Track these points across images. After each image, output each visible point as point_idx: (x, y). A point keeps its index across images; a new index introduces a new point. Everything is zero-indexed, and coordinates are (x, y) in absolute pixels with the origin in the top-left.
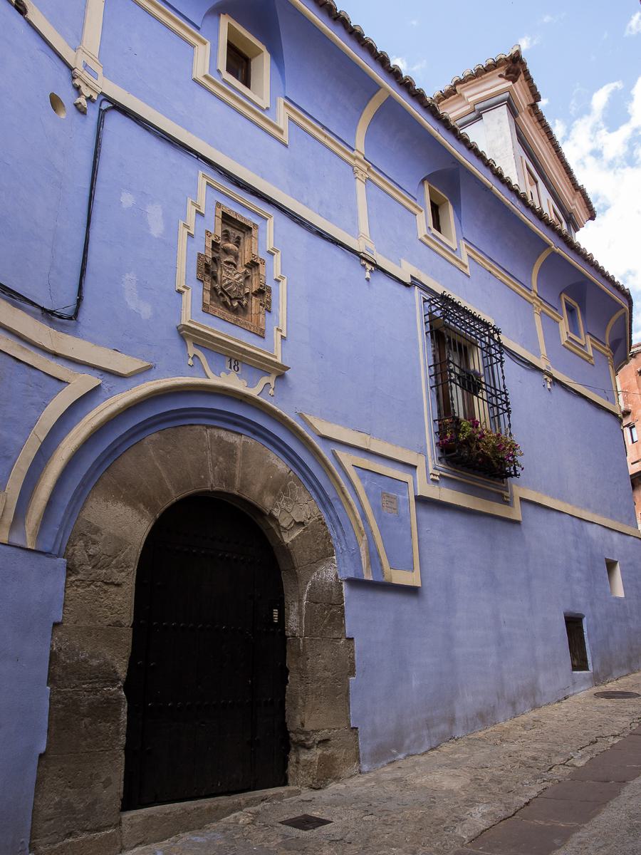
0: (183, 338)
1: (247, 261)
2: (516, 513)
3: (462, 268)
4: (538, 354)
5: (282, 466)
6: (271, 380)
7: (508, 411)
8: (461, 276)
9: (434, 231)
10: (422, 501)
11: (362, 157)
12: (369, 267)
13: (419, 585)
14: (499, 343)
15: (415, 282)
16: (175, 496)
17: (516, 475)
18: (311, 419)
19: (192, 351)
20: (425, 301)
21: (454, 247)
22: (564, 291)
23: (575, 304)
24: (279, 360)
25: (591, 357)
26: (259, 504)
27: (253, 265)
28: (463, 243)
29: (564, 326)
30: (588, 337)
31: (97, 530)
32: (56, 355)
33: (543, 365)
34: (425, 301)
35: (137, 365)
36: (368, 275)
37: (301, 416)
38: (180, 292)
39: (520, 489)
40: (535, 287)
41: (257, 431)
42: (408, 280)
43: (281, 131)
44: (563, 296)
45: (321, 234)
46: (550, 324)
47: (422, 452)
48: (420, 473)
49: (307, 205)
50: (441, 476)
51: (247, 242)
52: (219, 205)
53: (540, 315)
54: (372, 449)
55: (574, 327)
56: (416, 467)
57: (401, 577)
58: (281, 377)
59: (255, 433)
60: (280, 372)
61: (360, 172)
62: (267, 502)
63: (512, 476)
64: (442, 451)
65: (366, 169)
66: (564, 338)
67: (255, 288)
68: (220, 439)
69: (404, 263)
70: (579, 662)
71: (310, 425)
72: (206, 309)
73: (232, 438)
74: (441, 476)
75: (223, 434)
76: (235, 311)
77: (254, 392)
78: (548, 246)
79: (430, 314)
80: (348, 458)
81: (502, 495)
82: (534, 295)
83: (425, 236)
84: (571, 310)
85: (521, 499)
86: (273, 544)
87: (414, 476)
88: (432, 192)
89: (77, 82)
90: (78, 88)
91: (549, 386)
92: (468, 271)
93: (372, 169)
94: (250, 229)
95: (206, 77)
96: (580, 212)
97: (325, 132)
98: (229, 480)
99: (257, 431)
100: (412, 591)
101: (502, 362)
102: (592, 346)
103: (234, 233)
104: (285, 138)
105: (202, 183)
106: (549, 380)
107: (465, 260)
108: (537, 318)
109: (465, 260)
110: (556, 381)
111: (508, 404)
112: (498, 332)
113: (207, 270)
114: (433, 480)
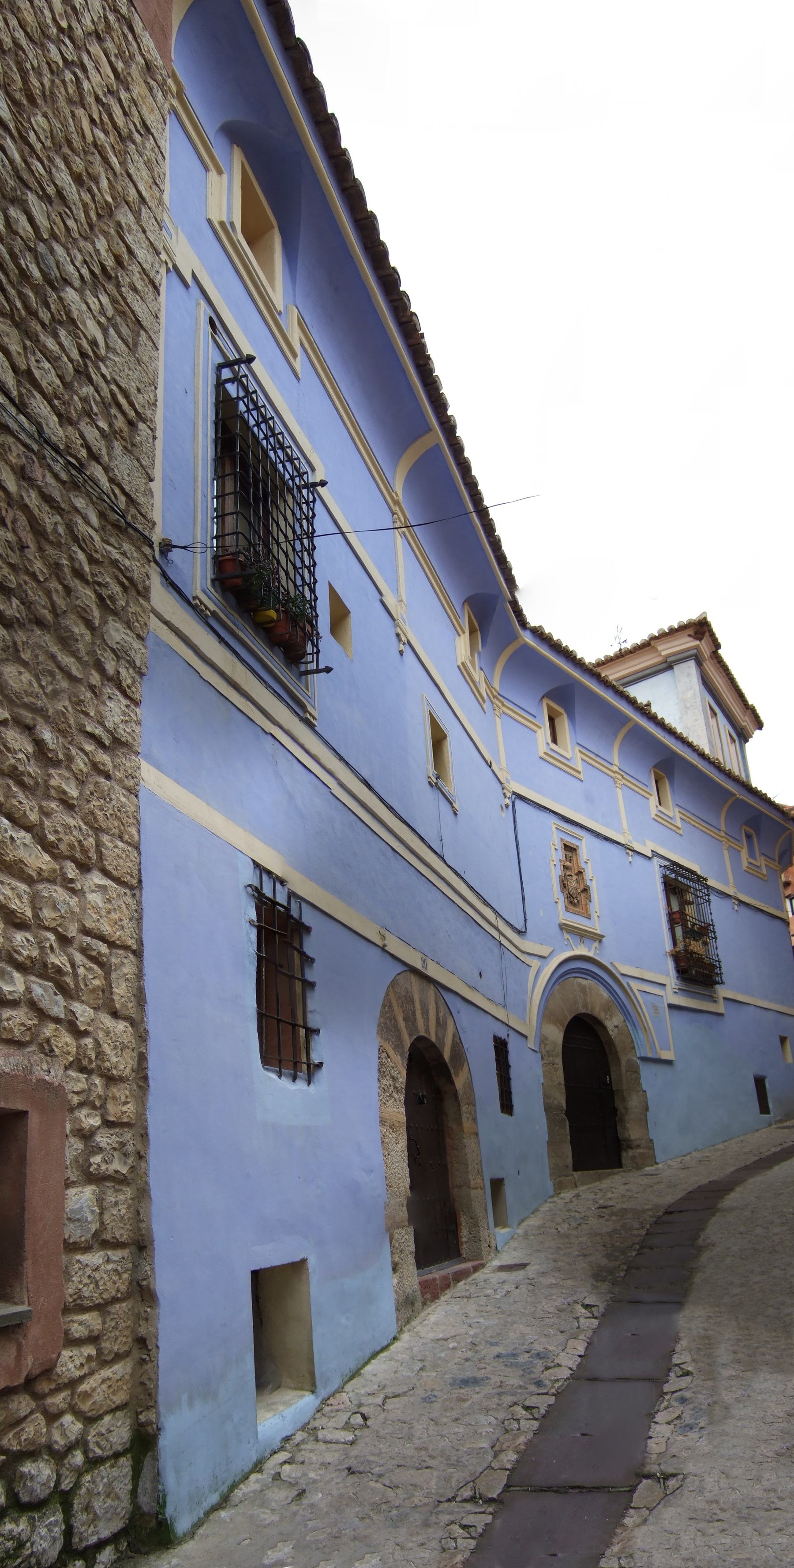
0: (561, 929)
1: (576, 871)
2: (721, 1008)
3: (678, 831)
4: (726, 883)
5: (605, 994)
6: (596, 944)
7: (715, 938)
8: (677, 836)
9: (660, 808)
10: (671, 1006)
11: (617, 769)
12: (631, 853)
13: (673, 1059)
14: (708, 887)
15: (655, 854)
16: (569, 1018)
17: (723, 983)
18: (616, 964)
19: (566, 936)
20: (661, 866)
21: (671, 815)
22: (746, 824)
23: (752, 831)
24: (598, 932)
25: (764, 875)
26: (599, 1018)
27: (580, 873)
28: (677, 809)
29: (744, 853)
30: (763, 858)
31: (547, 1039)
32: (523, 952)
33: (731, 891)
34: (661, 866)
35: (551, 949)
36: (630, 859)
37: (612, 963)
38: (556, 902)
39: (722, 992)
40: (723, 828)
41: (595, 976)
42: (650, 855)
43: (579, 772)
44: (744, 827)
45: (607, 839)
46: (735, 854)
47: (668, 975)
48: (668, 988)
49: (596, 821)
50: (679, 989)
51: (574, 859)
52: (562, 840)
53: (728, 850)
54: (645, 978)
55: (751, 854)
56: (665, 985)
57: (665, 1055)
58: (600, 941)
59: (593, 977)
60: (598, 938)
61: (619, 782)
62: (602, 1016)
63: (718, 983)
64: (678, 971)
65: (620, 777)
66: (745, 864)
67: (582, 888)
68: (580, 984)
69: (648, 843)
70: (764, 1108)
71: (616, 968)
72: (567, 910)
73: (584, 982)
74: (679, 989)
75: (580, 980)
76: (574, 905)
77: (590, 954)
78: (734, 795)
79: (665, 877)
80: (635, 986)
81: (712, 997)
82: (723, 834)
83: (656, 815)
84: (749, 837)
85: (725, 999)
86: (603, 1039)
87: (665, 990)
88: (656, 774)
89: (505, 791)
90: (504, 794)
91: (736, 908)
92: (681, 832)
93: (626, 776)
94: (575, 850)
95: (545, 753)
96: (745, 721)
97: (598, 759)
98: (585, 1006)
99: (595, 976)
100: (669, 1063)
101: (710, 902)
102: (766, 865)
103: (569, 854)
104: (581, 776)
105: (554, 827)
106: (737, 902)
107: (679, 823)
108: (726, 853)
109: (679, 824)
110: (741, 902)
111: (715, 932)
112: (706, 879)
113: (564, 886)
114: (675, 992)
